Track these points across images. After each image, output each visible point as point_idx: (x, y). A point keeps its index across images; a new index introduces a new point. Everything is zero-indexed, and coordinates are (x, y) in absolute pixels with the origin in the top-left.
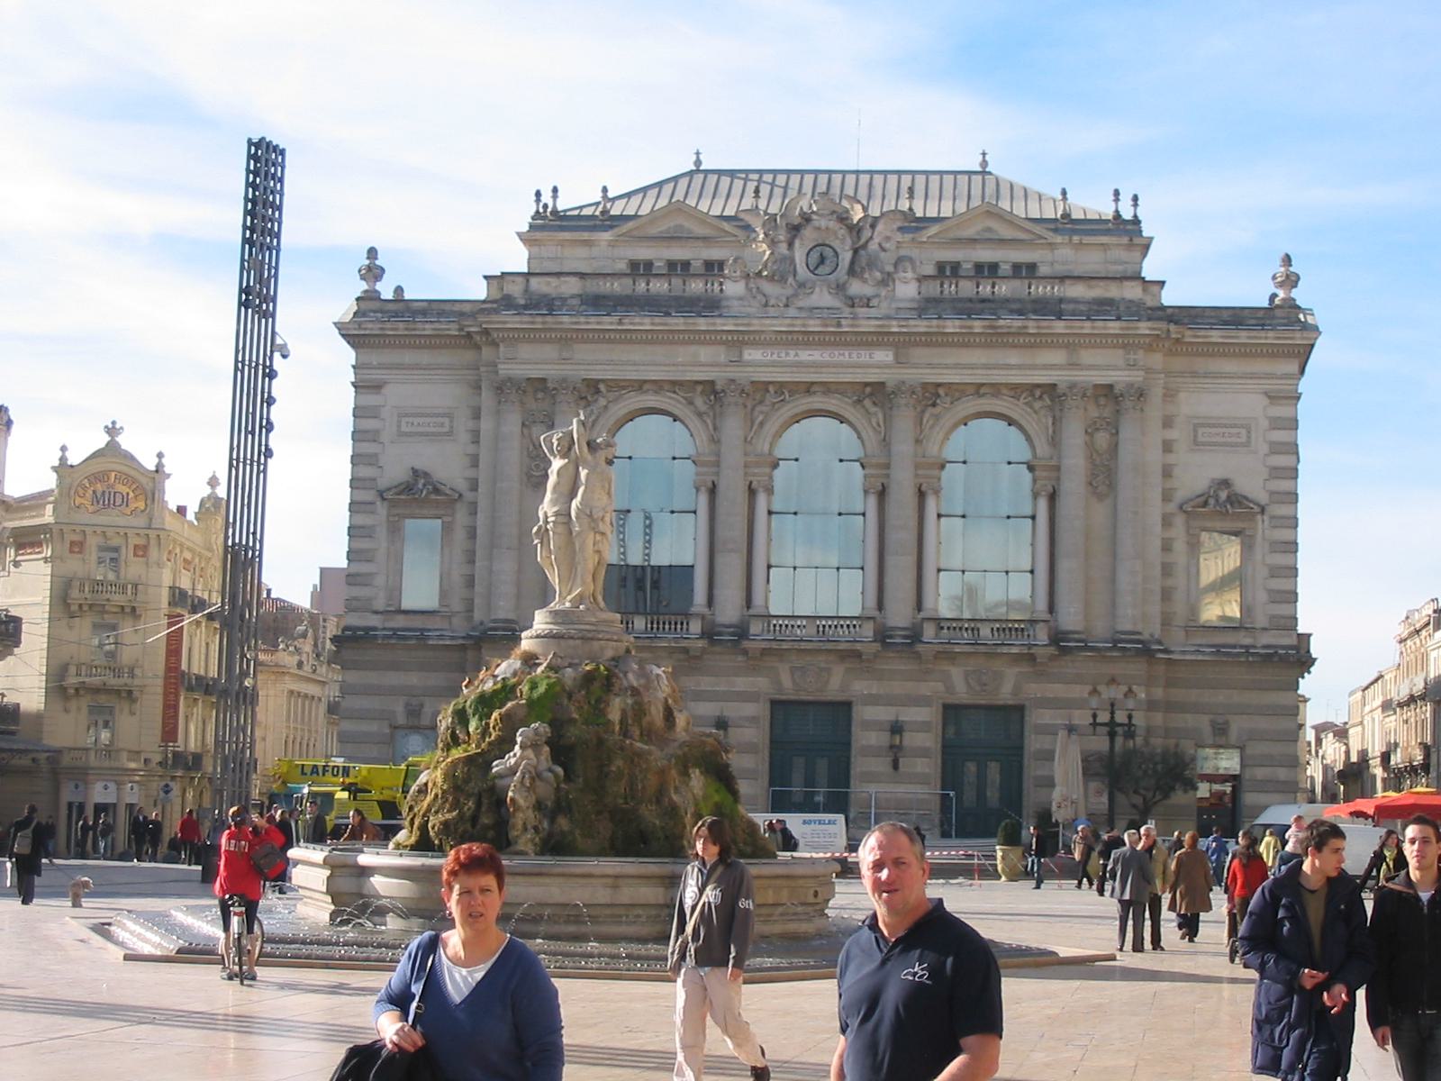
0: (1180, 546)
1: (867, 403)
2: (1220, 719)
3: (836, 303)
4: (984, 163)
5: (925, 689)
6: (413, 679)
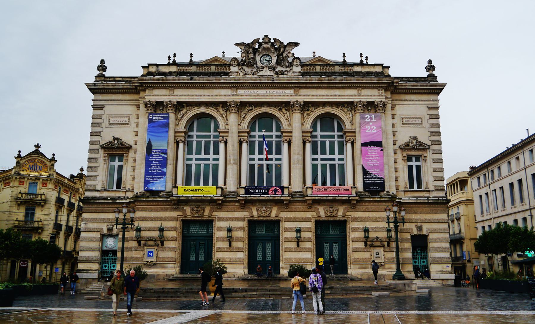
1: (284, 110)
2: (419, 224)
3: (272, 73)
5: (308, 215)
6: (112, 216)
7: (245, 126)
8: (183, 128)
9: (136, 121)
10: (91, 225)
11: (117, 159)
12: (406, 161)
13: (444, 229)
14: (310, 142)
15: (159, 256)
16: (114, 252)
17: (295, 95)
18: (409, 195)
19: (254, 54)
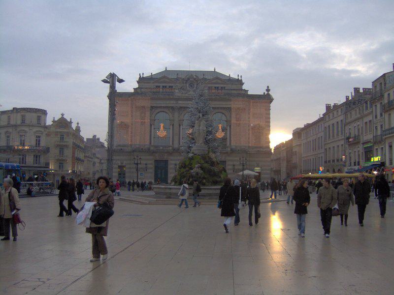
4: (215, 70)
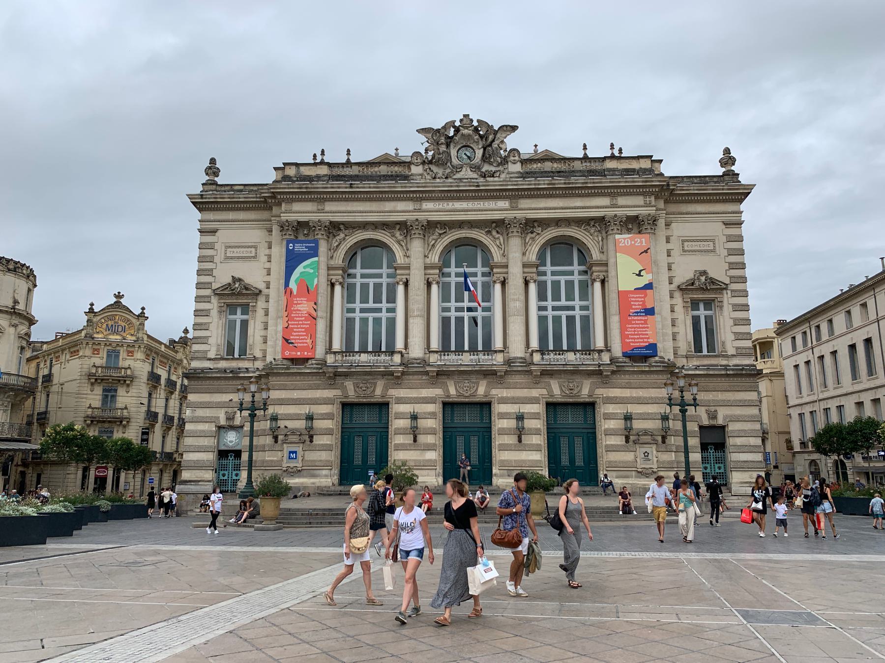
0: (679, 309)
1: (494, 233)
2: (713, 409)
3: (475, 176)
5: (535, 393)
7: (435, 258)
8: (340, 262)
9: (267, 252)
10: (200, 413)
11: (239, 311)
12: (690, 309)
13: (752, 416)
14: (535, 281)
15: (306, 458)
16: (238, 454)
17: (513, 208)
18: (695, 362)
19: (448, 146)
